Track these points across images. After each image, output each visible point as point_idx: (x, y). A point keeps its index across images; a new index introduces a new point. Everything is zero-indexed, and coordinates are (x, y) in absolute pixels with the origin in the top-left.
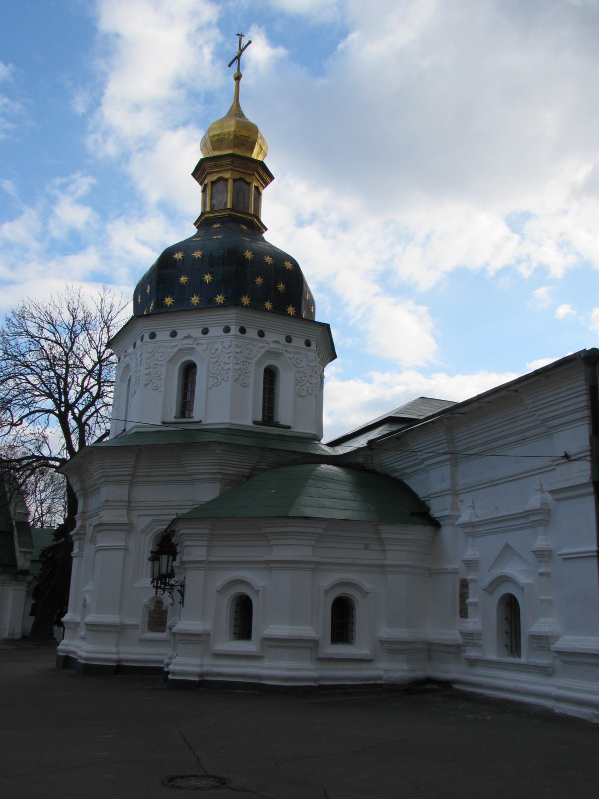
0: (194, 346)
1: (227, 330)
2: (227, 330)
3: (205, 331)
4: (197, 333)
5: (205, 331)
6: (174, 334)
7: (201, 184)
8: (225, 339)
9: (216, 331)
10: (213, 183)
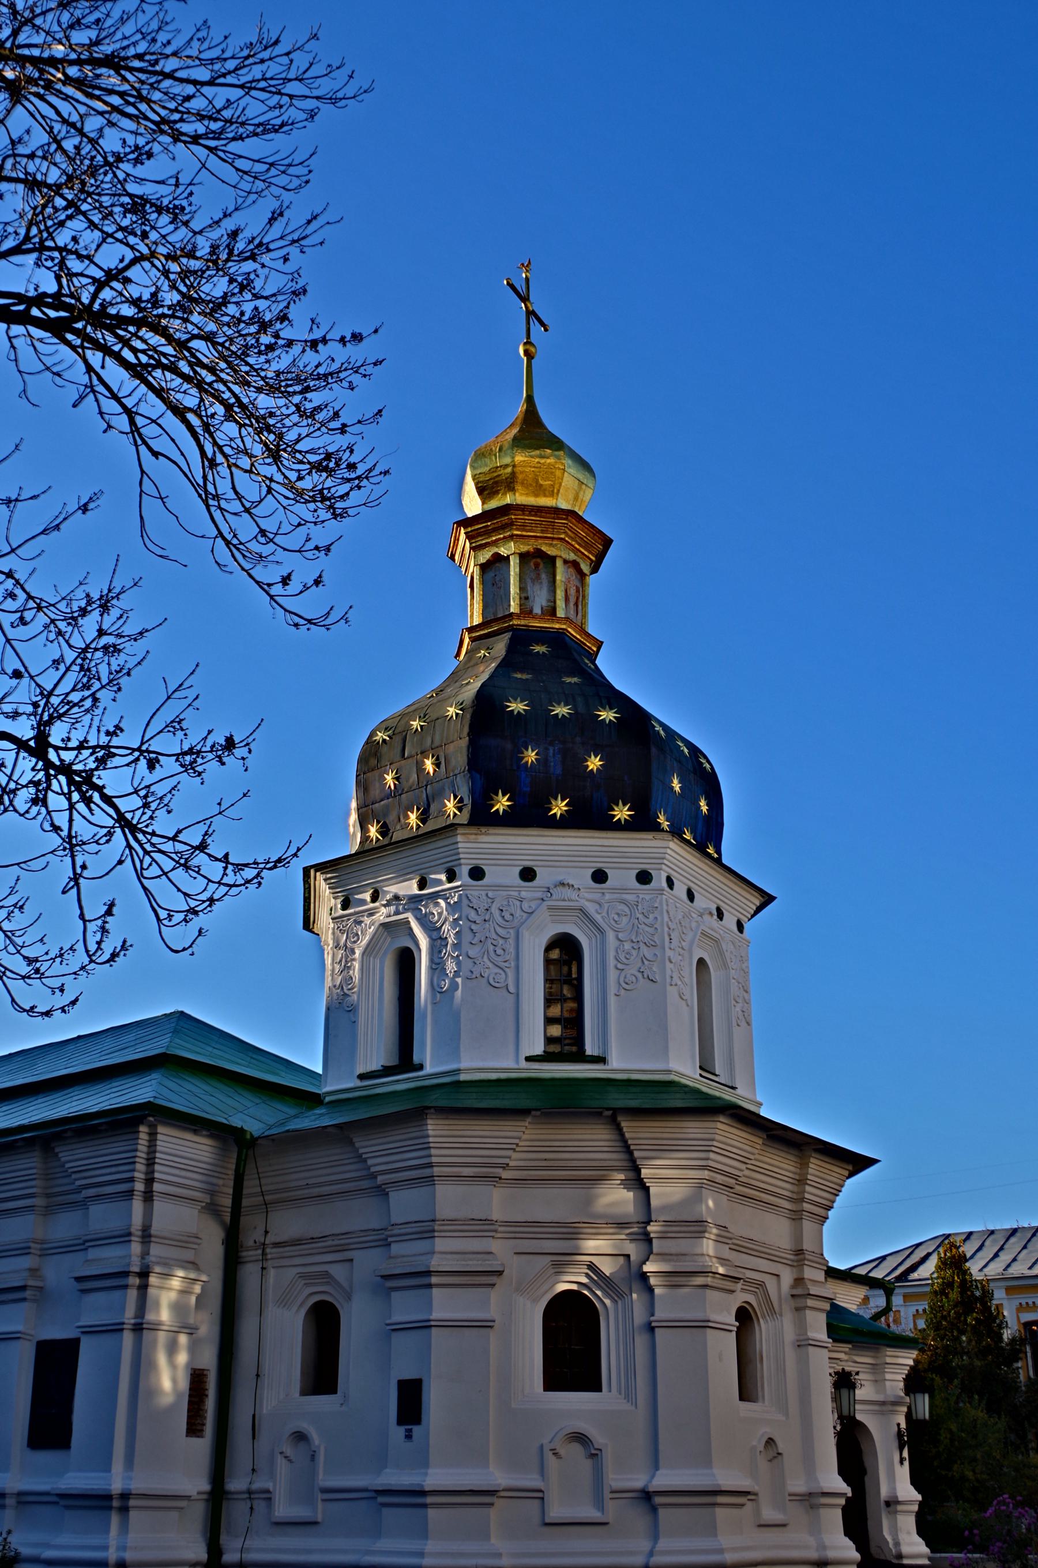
3: (599, 876)
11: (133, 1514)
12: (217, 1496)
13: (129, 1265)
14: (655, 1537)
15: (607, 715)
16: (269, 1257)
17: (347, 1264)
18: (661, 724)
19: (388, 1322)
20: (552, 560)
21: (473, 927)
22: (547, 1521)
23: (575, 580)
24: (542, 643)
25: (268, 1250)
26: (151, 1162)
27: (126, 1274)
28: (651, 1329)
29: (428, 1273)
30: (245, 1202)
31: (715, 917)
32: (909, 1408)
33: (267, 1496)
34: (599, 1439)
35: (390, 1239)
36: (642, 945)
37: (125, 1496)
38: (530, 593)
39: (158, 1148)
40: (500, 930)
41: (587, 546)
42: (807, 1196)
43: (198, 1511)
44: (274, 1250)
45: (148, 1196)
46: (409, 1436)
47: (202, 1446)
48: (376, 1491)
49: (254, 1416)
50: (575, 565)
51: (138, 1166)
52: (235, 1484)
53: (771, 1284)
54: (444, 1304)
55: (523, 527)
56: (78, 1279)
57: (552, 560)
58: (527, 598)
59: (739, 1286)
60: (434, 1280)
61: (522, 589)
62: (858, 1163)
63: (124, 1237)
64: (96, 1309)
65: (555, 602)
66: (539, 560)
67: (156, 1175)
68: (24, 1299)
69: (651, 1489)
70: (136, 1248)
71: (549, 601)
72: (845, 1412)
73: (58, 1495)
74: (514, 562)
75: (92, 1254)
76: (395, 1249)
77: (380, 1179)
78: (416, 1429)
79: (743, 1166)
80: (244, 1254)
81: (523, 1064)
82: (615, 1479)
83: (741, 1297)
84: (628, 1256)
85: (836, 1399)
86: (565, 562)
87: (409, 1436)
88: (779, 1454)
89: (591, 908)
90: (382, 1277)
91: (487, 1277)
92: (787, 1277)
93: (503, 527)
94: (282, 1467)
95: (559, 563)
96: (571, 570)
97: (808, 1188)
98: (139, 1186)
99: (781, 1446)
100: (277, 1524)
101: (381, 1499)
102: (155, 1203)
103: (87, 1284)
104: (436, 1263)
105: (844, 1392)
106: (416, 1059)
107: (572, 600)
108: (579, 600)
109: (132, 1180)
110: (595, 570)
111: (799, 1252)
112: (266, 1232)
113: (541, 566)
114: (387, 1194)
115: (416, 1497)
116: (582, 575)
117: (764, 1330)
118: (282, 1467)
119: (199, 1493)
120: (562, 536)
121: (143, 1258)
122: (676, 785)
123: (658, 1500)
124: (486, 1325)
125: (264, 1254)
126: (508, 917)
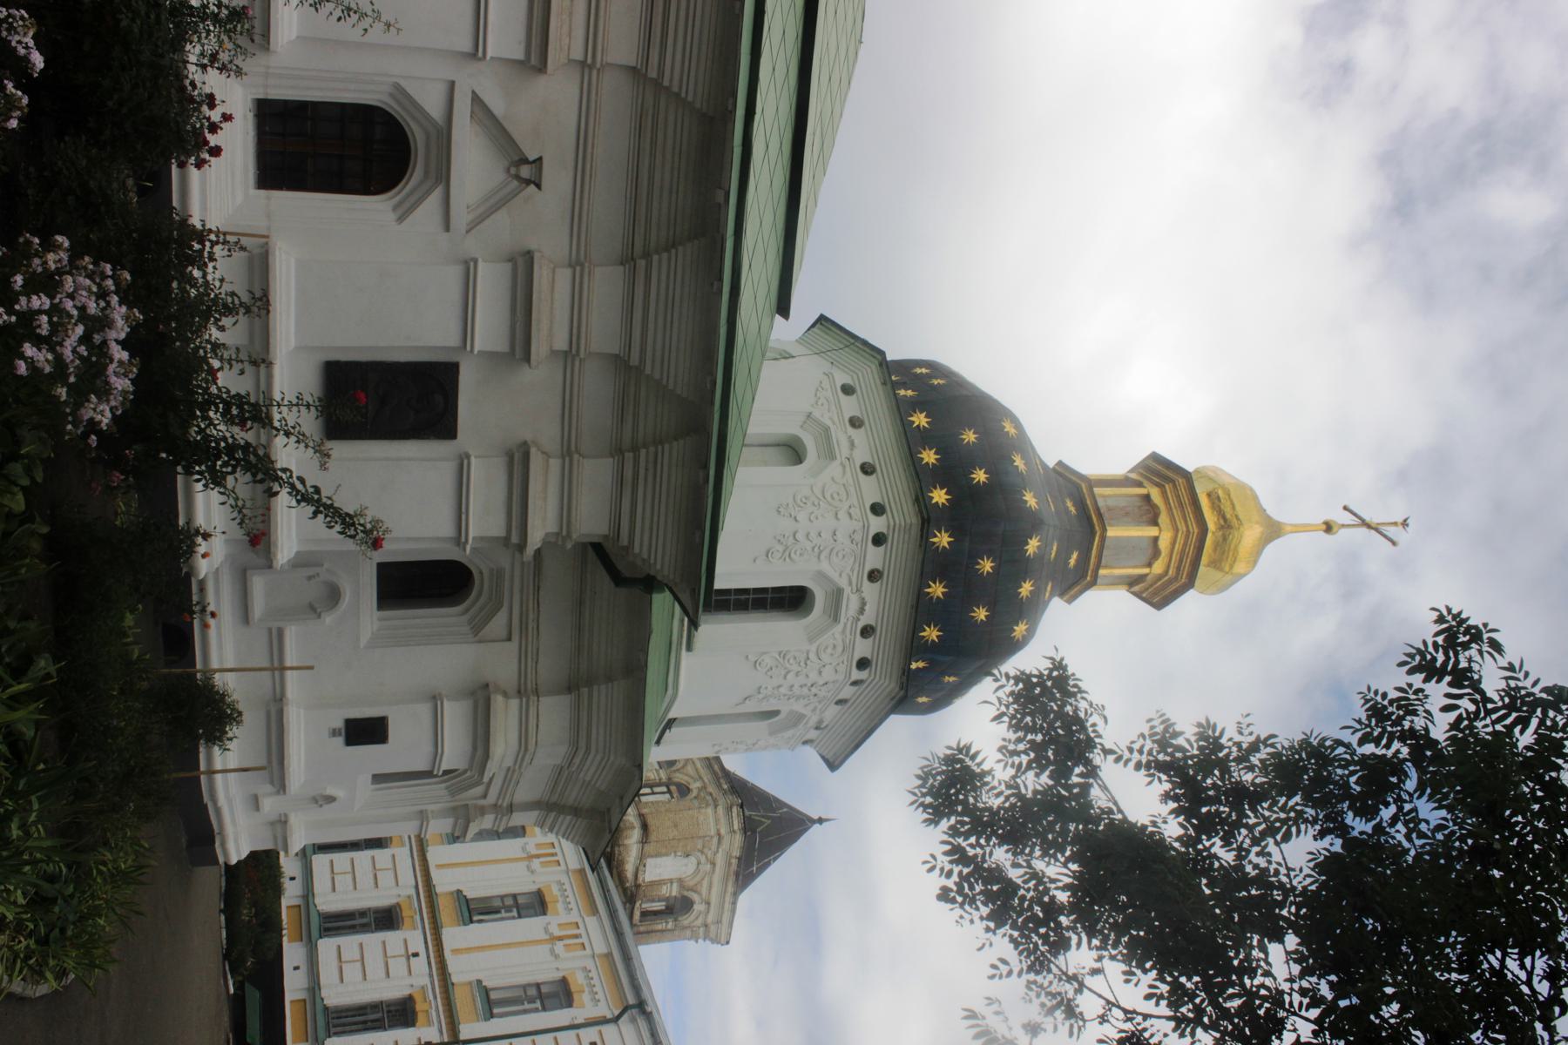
10: (1156, 539)
17: (504, 634)
46: (334, 733)
55: (1170, 582)
74: (1146, 571)
78: (340, 740)
84: (485, 796)
87: (334, 733)
93: (1178, 568)
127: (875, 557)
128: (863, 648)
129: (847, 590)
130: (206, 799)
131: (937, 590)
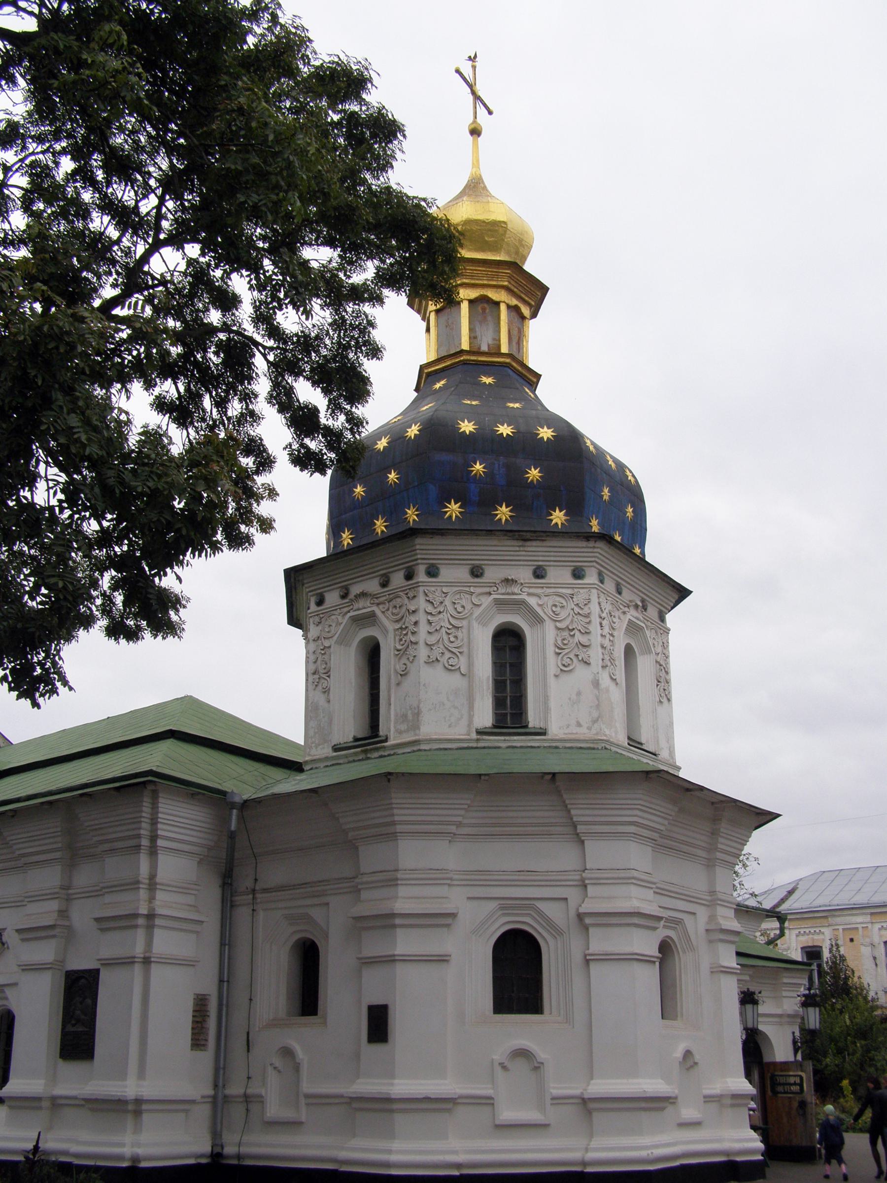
0: (524, 596)
1: (578, 574)
2: (578, 574)
3: (539, 573)
4: (524, 574)
5: (539, 573)
6: (476, 572)
7: (419, 312)
8: (576, 590)
9: (559, 575)
11: (145, 1116)
12: (219, 1102)
13: (138, 908)
14: (591, 1140)
15: (546, 433)
16: (259, 900)
18: (593, 443)
19: (360, 956)
20: (497, 304)
21: (430, 618)
22: (497, 1122)
23: (516, 319)
24: (488, 375)
25: (258, 895)
26: (154, 822)
27: (135, 916)
28: (587, 962)
29: (393, 915)
30: (237, 855)
31: (640, 608)
32: (803, 1019)
33: (260, 1099)
34: (542, 1055)
35: (360, 887)
36: (577, 633)
37: (139, 1101)
38: (478, 334)
39: (160, 810)
40: (453, 621)
41: (529, 293)
42: (720, 846)
43: (203, 1112)
44: (264, 895)
45: (153, 851)
47: (207, 1057)
48: (351, 1098)
49: (248, 1033)
50: (516, 309)
51: (144, 825)
52: (235, 1089)
53: (688, 920)
54: (406, 943)
56: (98, 920)
57: (497, 304)
58: (475, 338)
59: (662, 923)
60: (398, 921)
61: (471, 330)
62: (763, 817)
63: (134, 885)
64: (111, 946)
65: (499, 341)
66: (486, 305)
67: (159, 832)
68: (54, 936)
69: (586, 1096)
70: (143, 894)
71: (494, 339)
72: (750, 1025)
73: (84, 1099)
75: (108, 899)
76: (364, 895)
77: (350, 834)
79: (666, 822)
80: (237, 898)
81: (474, 736)
82: (556, 1089)
83: (662, 933)
84: (566, 899)
85: (743, 1014)
86: (509, 307)
88: (696, 1063)
89: (533, 601)
90: (354, 918)
91: (443, 920)
92: (703, 914)
94: (273, 1078)
95: (503, 307)
96: (514, 314)
97: (720, 840)
98: (145, 842)
99: (697, 1058)
100: (267, 1123)
101: (355, 1105)
102: (159, 856)
103: (106, 924)
104: (401, 906)
105: (749, 1007)
106: (382, 732)
107: (515, 340)
108: (518, 338)
109: (139, 836)
110: (534, 315)
111: (712, 893)
112: (256, 880)
113: (487, 311)
114: (357, 848)
115: (385, 1105)
116: (523, 318)
117: (684, 961)
118: (273, 1078)
119: (203, 1097)
120: (506, 283)
121: (150, 902)
122: (606, 493)
123: (591, 1105)
124: (442, 959)
125: (254, 898)
126: (460, 609)
127: (332, 598)
128: (398, 579)
129: (352, 614)
130: (456, 1173)
131: (380, 526)
